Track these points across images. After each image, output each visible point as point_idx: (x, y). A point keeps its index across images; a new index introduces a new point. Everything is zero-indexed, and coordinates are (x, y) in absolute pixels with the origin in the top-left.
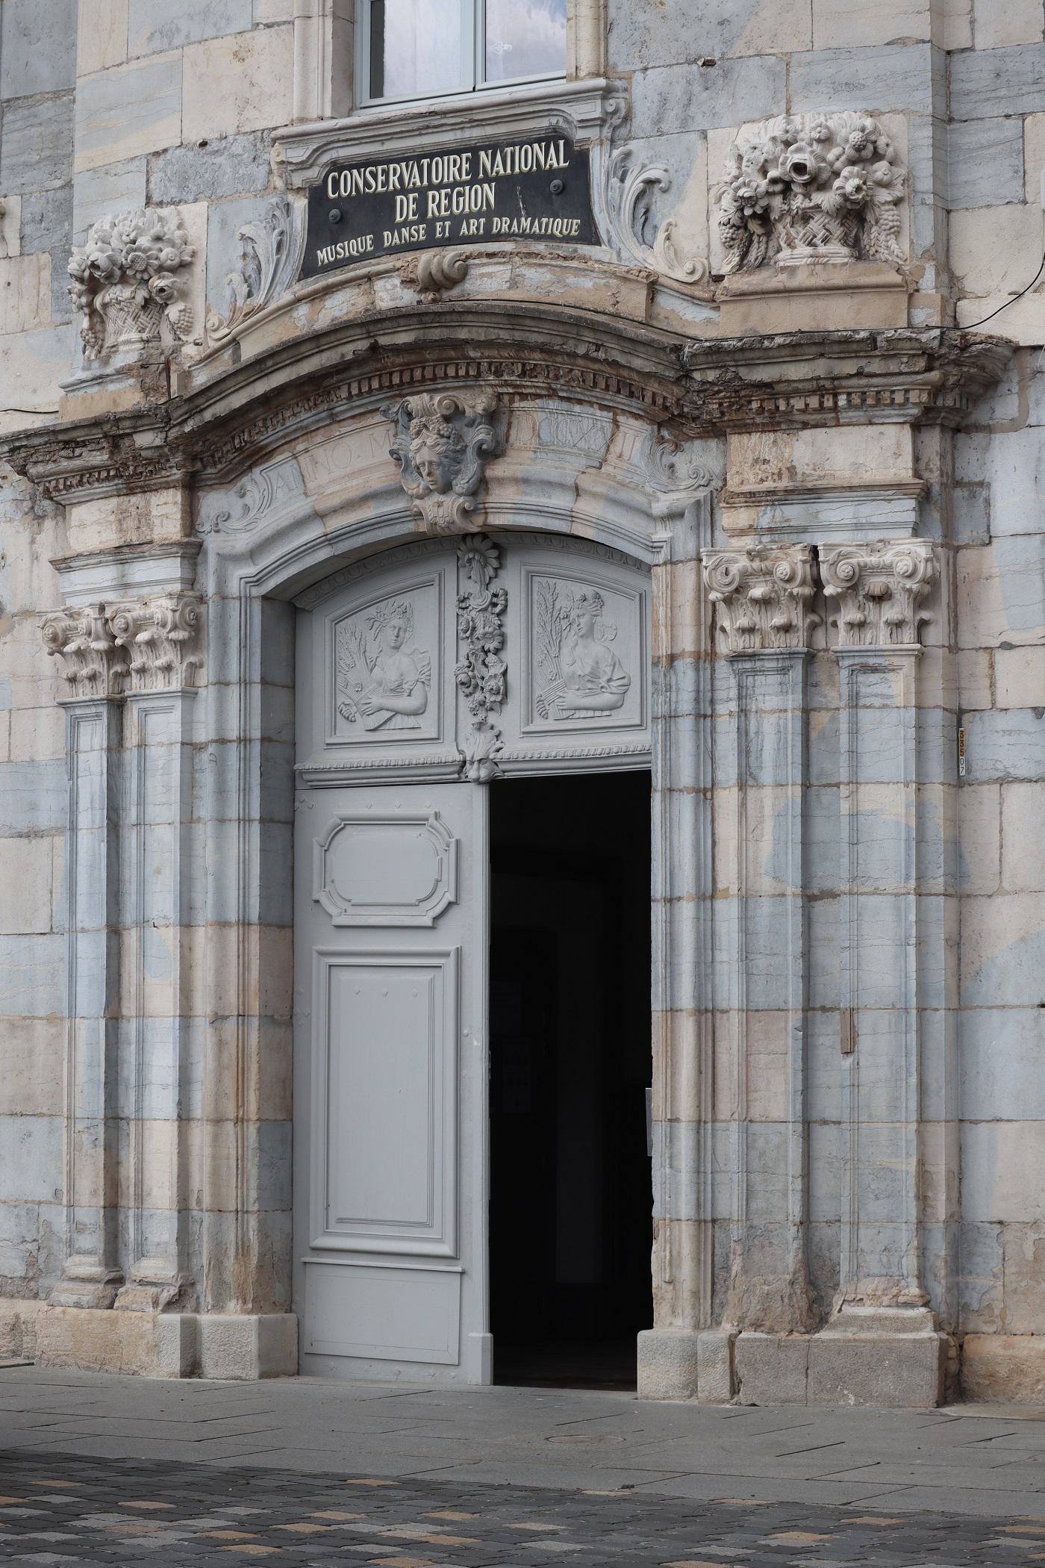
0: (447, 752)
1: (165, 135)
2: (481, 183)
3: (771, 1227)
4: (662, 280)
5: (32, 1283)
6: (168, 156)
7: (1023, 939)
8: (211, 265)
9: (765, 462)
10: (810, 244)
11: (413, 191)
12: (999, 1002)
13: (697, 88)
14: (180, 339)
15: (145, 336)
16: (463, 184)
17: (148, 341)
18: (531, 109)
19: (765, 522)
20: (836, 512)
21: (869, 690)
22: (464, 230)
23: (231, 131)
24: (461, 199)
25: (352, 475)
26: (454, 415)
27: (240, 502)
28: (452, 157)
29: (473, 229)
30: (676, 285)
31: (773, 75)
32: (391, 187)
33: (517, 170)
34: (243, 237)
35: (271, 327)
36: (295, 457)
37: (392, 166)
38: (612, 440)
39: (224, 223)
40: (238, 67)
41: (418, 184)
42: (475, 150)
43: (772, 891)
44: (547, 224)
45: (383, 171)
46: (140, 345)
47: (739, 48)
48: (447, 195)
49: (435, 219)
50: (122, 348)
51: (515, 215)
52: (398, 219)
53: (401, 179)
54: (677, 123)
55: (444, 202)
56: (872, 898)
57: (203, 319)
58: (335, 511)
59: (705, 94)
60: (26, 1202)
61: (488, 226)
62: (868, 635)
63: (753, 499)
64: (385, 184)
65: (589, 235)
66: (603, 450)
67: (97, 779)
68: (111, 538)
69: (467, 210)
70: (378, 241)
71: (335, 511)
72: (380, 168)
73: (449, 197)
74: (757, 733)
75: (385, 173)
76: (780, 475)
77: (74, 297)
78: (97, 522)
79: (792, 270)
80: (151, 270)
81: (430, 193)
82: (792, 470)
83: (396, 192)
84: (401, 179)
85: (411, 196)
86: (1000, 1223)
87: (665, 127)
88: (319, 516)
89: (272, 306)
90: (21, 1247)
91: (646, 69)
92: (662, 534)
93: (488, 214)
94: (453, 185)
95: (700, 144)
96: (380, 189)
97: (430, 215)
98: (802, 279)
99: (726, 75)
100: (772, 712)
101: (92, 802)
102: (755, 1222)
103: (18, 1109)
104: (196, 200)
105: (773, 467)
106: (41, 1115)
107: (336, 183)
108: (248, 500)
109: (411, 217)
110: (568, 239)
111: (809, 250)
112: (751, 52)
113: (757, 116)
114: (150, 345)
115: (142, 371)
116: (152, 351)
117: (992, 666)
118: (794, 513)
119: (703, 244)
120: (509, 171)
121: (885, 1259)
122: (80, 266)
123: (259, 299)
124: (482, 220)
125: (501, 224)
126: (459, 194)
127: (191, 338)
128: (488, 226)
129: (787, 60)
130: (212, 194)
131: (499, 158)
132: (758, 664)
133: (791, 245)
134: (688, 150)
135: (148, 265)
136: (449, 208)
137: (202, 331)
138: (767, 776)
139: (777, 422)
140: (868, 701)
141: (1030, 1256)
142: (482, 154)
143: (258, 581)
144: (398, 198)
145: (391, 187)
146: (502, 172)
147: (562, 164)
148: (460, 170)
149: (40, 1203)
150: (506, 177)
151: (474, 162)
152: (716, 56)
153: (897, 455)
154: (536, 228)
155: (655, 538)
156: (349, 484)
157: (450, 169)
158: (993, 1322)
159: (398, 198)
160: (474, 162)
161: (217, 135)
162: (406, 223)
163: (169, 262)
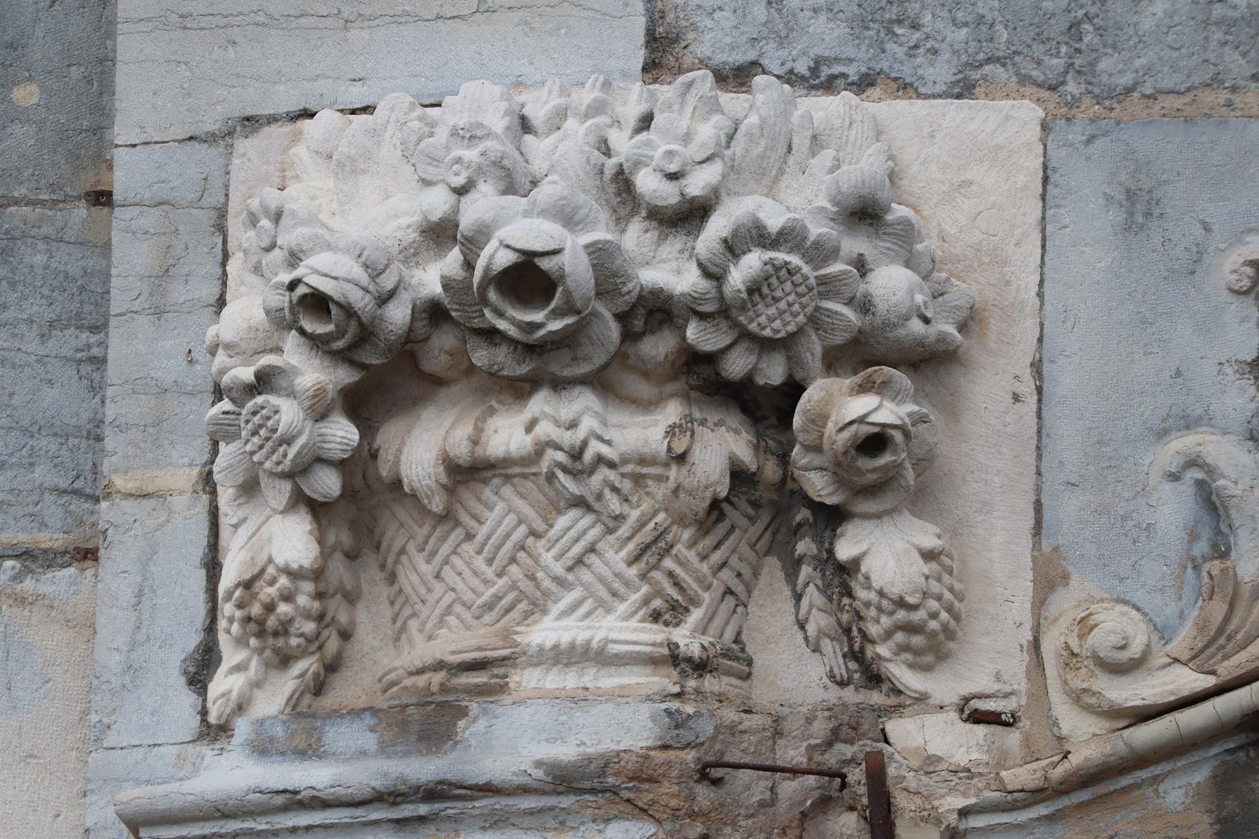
8: (1062, 379)
14: (874, 678)
15: (687, 638)
17: (701, 667)
46: (665, 681)
50: (527, 679)
57: (1021, 609)
77: (288, 413)
80: (813, 349)
104: (963, 89)
114: (710, 683)
115: (704, 795)
116: (730, 715)
122: (375, 272)
135: (815, 320)
137: (1016, 670)
163: (916, 326)
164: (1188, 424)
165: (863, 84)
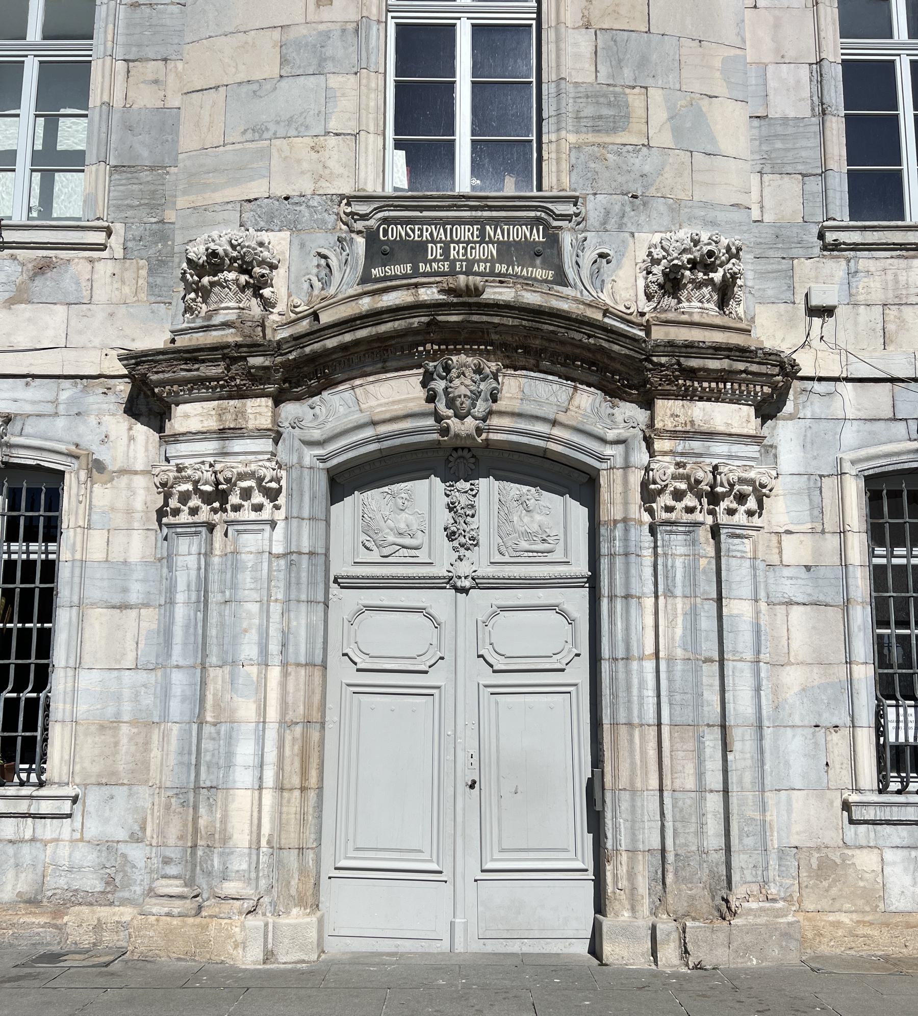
0: (440, 570)
1: (257, 189)
2: (487, 243)
3: (689, 855)
4: (611, 309)
5: (109, 896)
6: (258, 202)
7: (803, 690)
8: (292, 269)
9: (677, 416)
10: (700, 301)
11: (439, 242)
12: (790, 724)
13: (628, 209)
16: (475, 242)
18: (527, 204)
19: (680, 449)
20: (720, 448)
21: (734, 548)
22: (476, 268)
23: (309, 192)
24: (474, 251)
25: (394, 403)
26: (478, 370)
27: (312, 411)
28: (467, 227)
29: (482, 269)
30: (621, 314)
31: (671, 209)
32: (424, 239)
33: (511, 239)
34: (319, 254)
35: (342, 307)
36: (353, 388)
37: (425, 227)
38: (571, 398)
39: (302, 245)
40: (314, 155)
41: (444, 238)
42: (482, 223)
43: (683, 657)
44: (532, 272)
45: (419, 229)
47: (652, 191)
48: (463, 247)
49: (455, 260)
51: (510, 263)
52: (429, 257)
53: (431, 234)
54: (617, 226)
55: (461, 251)
56: (739, 663)
58: (384, 422)
59: (633, 213)
60: (107, 841)
61: (493, 268)
62: (737, 516)
63: (674, 434)
64: (421, 236)
65: (561, 279)
66: (567, 403)
67: (193, 573)
68: (212, 424)
69: (477, 257)
70: (415, 268)
71: (384, 422)
72: (417, 227)
73: (465, 249)
74: (672, 567)
75: (421, 230)
76: (686, 424)
78: (200, 415)
79: (691, 314)
81: (452, 245)
82: (692, 422)
83: (427, 242)
84: (431, 234)
85: (439, 245)
86: (796, 847)
87: (608, 227)
88: (374, 423)
89: (340, 296)
90: (101, 871)
91: (595, 194)
92: (608, 451)
93: (493, 262)
94: (468, 242)
95: (630, 240)
96: (416, 238)
97: (452, 257)
98: (696, 318)
99: (645, 204)
100: (681, 555)
101: (188, 586)
102: (679, 852)
103: (104, 781)
104: (280, 231)
105: (682, 419)
106: (123, 784)
107: (386, 232)
108: (317, 410)
109: (438, 257)
110: (546, 281)
111: (700, 305)
112: (659, 195)
113: (663, 229)
117: (780, 543)
118: (696, 445)
119: (632, 292)
120: (506, 239)
121: (754, 873)
123: (332, 290)
124: (488, 264)
125: (501, 268)
126: (472, 248)
127: (274, 311)
128: (493, 268)
129: (678, 201)
130: (293, 227)
131: (499, 230)
132: (674, 528)
133: (688, 300)
134: (623, 241)
136: (465, 254)
137: (285, 308)
138: (678, 591)
139: (688, 395)
140: (734, 554)
141: (815, 866)
142: (488, 227)
143: (323, 460)
144: (430, 245)
145: (424, 239)
146: (501, 239)
147: (541, 239)
148: (472, 234)
149: (118, 842)
150: (503, 243)
151: (482, 232)
152: (639, 193)
153: (748, 421)
154: (525, 272)
155: (606, 453)
156: (392, 408)
157: (465, 233)
158: (793, 905)
159: (430, 245)
160: (482, 232)
161: (298, 194)
162: (435, 260)
164: (308, 274)
165: (267, 231)
